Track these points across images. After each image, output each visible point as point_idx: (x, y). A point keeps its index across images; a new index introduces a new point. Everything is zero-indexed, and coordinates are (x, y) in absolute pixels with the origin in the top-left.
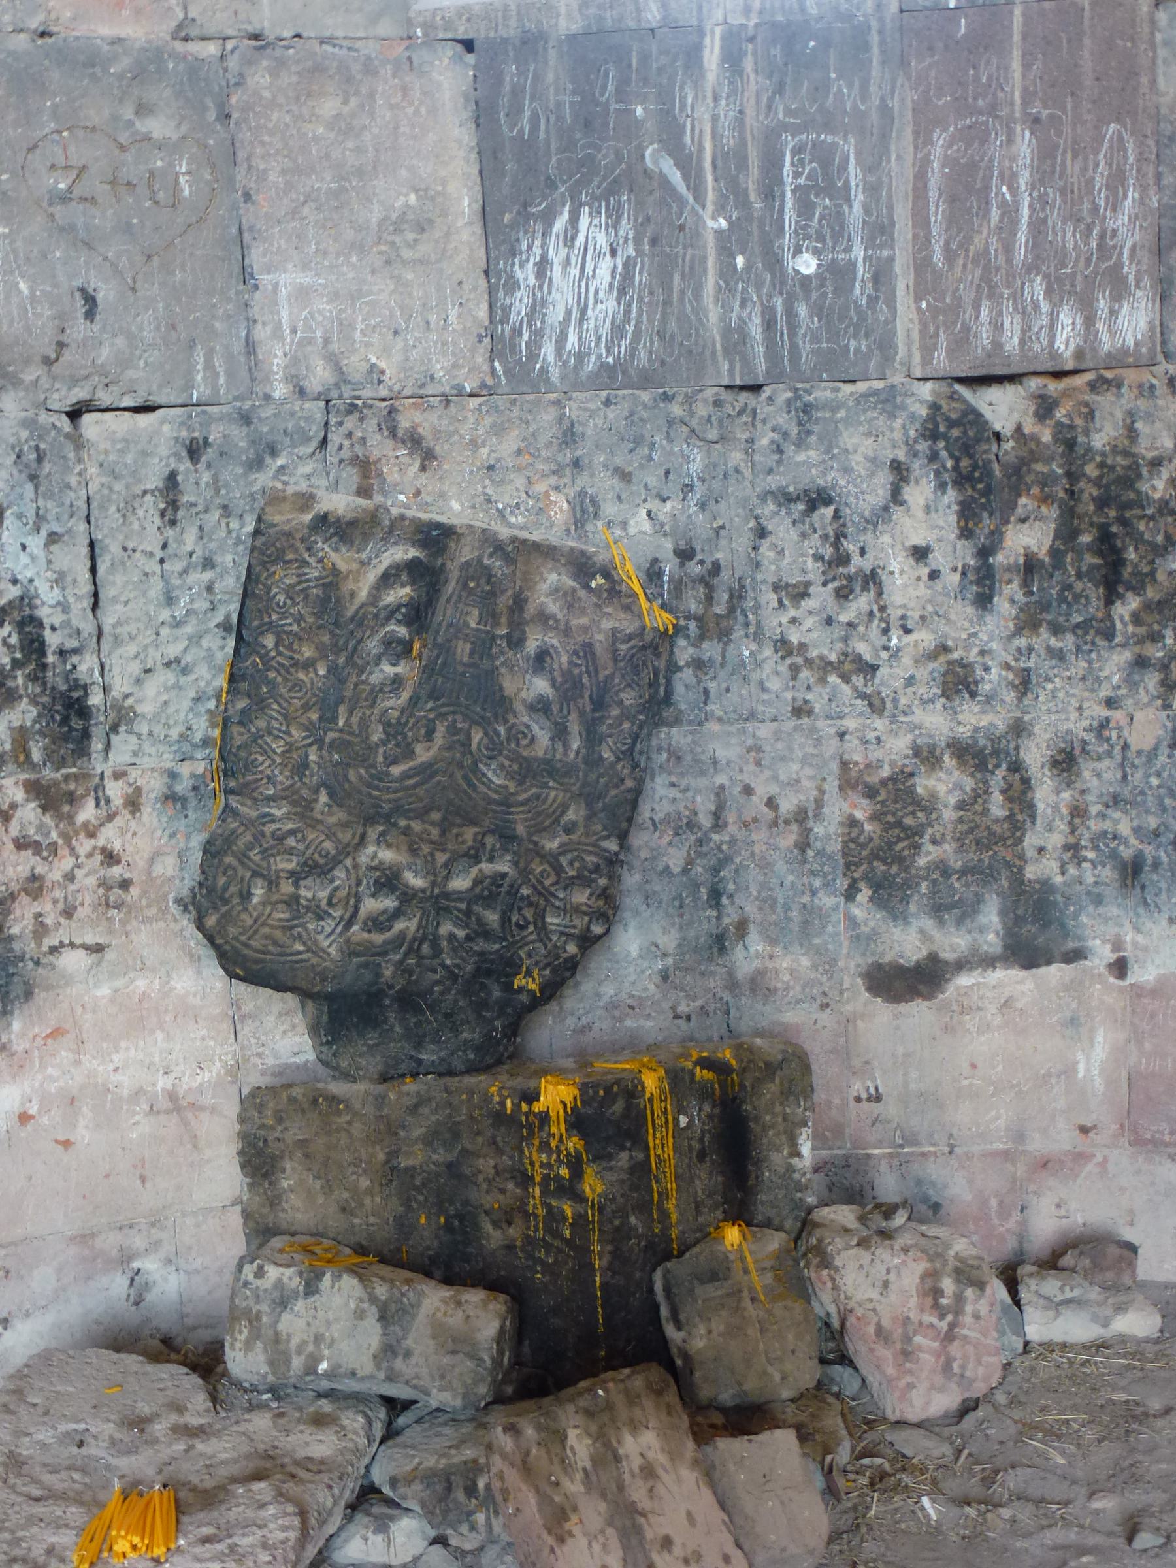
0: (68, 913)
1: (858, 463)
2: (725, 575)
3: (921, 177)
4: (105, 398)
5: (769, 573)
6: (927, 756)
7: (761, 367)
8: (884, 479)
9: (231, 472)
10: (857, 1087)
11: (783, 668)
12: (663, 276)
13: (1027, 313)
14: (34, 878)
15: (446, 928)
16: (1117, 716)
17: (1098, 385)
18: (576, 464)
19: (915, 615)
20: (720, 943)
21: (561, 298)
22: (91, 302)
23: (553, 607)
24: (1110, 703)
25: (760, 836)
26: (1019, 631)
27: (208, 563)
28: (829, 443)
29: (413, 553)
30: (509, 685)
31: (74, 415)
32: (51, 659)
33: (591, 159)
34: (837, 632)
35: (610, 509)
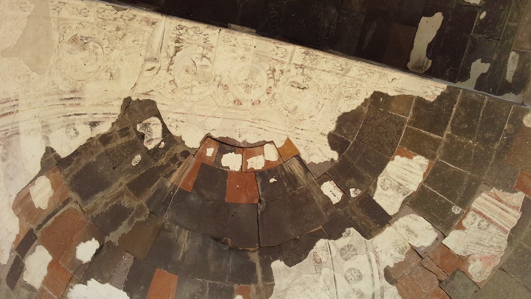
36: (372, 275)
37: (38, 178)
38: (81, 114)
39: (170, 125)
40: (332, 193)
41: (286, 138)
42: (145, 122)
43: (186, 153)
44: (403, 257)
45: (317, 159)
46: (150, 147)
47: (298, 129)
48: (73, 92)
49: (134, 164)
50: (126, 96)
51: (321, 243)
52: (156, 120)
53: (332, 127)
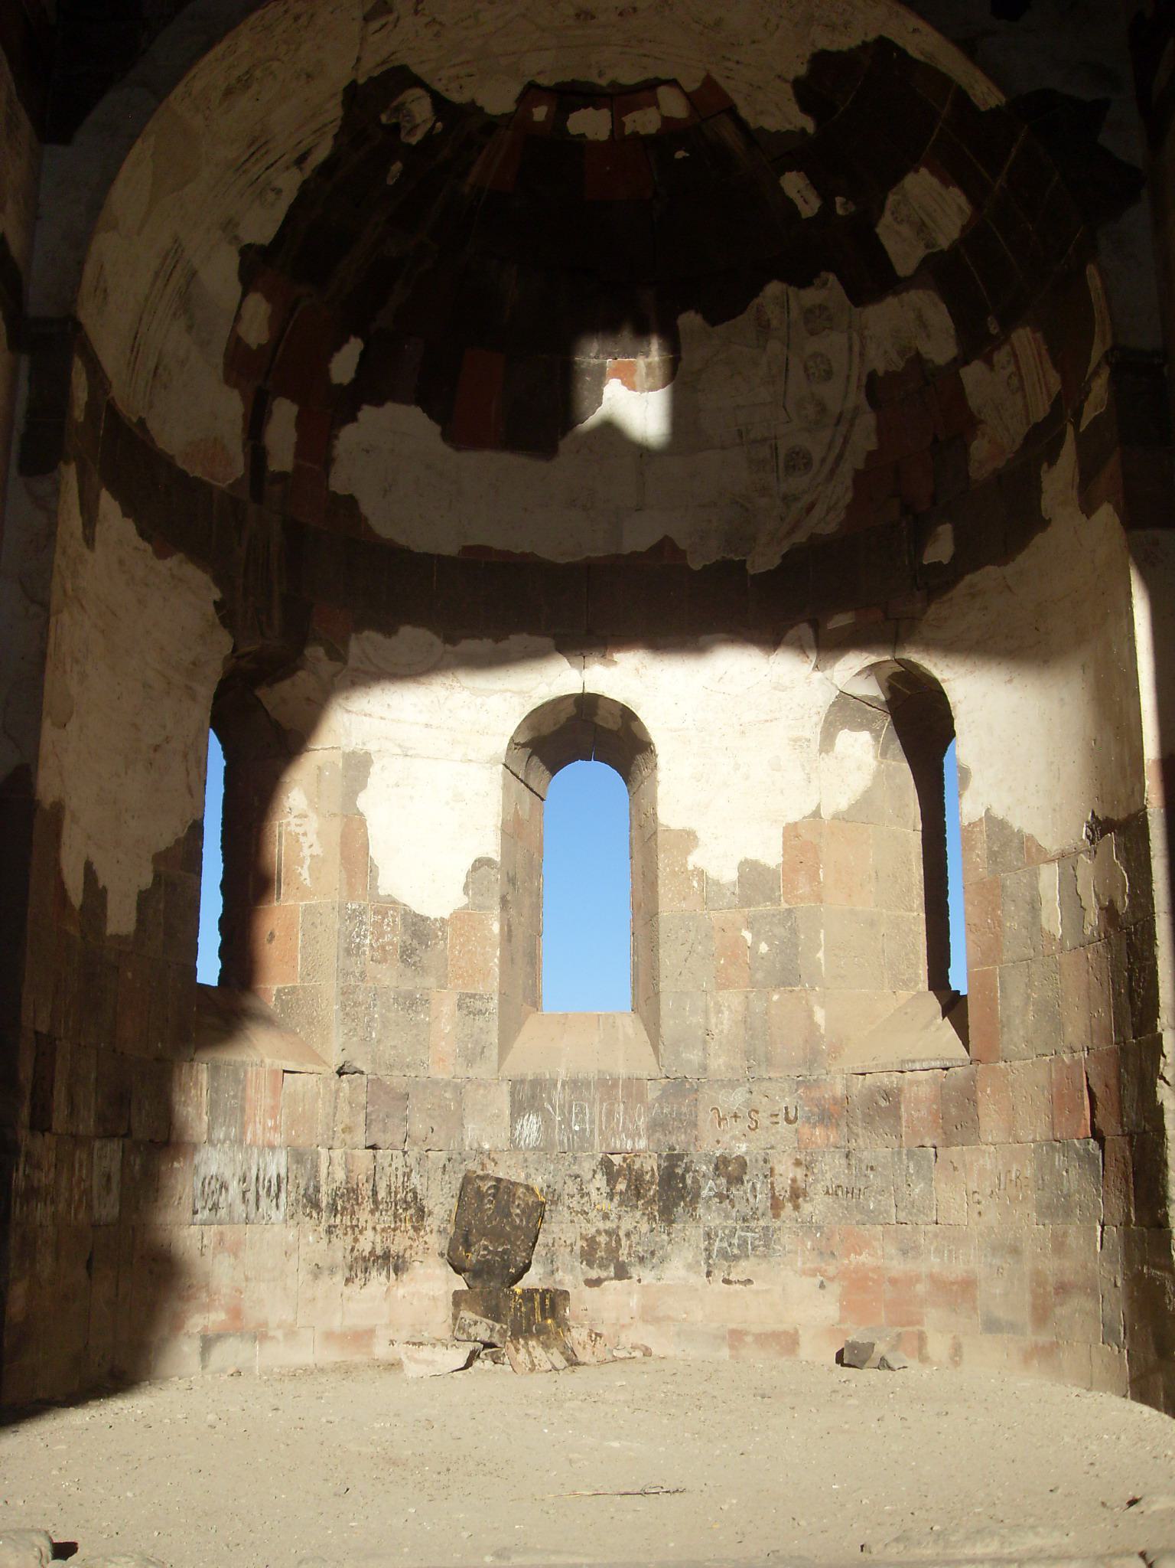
0: (417, 1254)
1: (586, 1170)
2: (557, 1192)
3: (601, 1112)
4: (433, 1148)
5: (566, 1192)
6: (598, 1232)
7: (566, 1148)
8: (592, 1173)
9: (456, 1164)
10: (582, 1307)
11: (569, 1212)
12: (546, 1129)
13: (621, 1140)
14: (411, 1245)
15: (497, 1258)
16: (639, 1225)
17: (635, 1156)
18: (527, 1167)
19: (597, 1202)
20: (552, 1272)
21: (526, 1132)
22: (433, 1129)
23: (521, 1195)
24: (637, 1222)
25: (562, 1248)
26: (619, 1206)
27: (450, 1183)
28: (580, 1165)
29: (494, 1183)
30: (512, 1211)
31: (426, 1151)
32: (418, 1200)
33: (533, 1105)
34: (580, 1205)
35: (533, 1176)
36: (848, 377)
37: (244, 304)
38: (276, 162)
39: (447, 90)
40: (802, 197)
41: (703, 75)
42: (395, 104)
43: (492, 125)
44: (902, 364)
45: (772, 123)
46: (414, 140)
47: (729, 59)
48: (249, 147)
49: (390, 182)
50: (346, 83)
51: (774, 288)
52: (418, 92)
53: (802, 70)
